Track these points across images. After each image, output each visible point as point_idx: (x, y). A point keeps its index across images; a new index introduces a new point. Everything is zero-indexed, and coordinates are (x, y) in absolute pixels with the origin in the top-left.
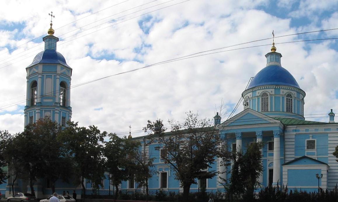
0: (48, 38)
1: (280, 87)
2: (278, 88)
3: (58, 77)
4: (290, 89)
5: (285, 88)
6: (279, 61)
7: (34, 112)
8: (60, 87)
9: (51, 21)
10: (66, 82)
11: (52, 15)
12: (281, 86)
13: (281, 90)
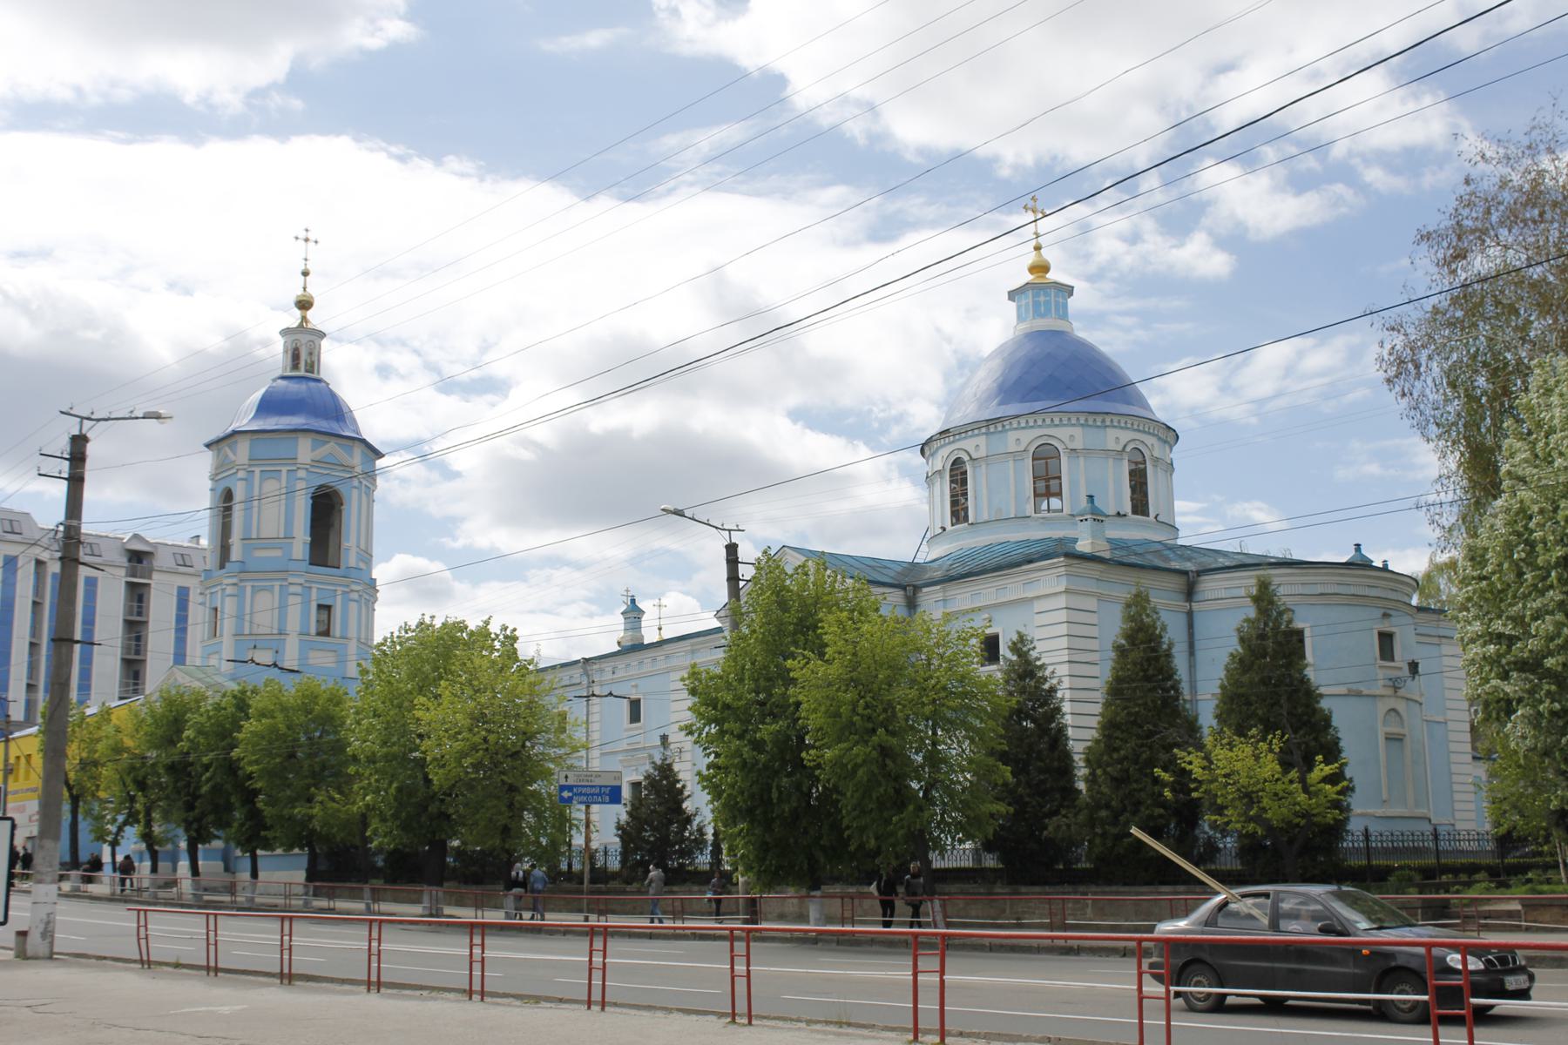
2: (1000, 429)
5: (1023, 425)
6: (1063, 314)
7: (219, 593)
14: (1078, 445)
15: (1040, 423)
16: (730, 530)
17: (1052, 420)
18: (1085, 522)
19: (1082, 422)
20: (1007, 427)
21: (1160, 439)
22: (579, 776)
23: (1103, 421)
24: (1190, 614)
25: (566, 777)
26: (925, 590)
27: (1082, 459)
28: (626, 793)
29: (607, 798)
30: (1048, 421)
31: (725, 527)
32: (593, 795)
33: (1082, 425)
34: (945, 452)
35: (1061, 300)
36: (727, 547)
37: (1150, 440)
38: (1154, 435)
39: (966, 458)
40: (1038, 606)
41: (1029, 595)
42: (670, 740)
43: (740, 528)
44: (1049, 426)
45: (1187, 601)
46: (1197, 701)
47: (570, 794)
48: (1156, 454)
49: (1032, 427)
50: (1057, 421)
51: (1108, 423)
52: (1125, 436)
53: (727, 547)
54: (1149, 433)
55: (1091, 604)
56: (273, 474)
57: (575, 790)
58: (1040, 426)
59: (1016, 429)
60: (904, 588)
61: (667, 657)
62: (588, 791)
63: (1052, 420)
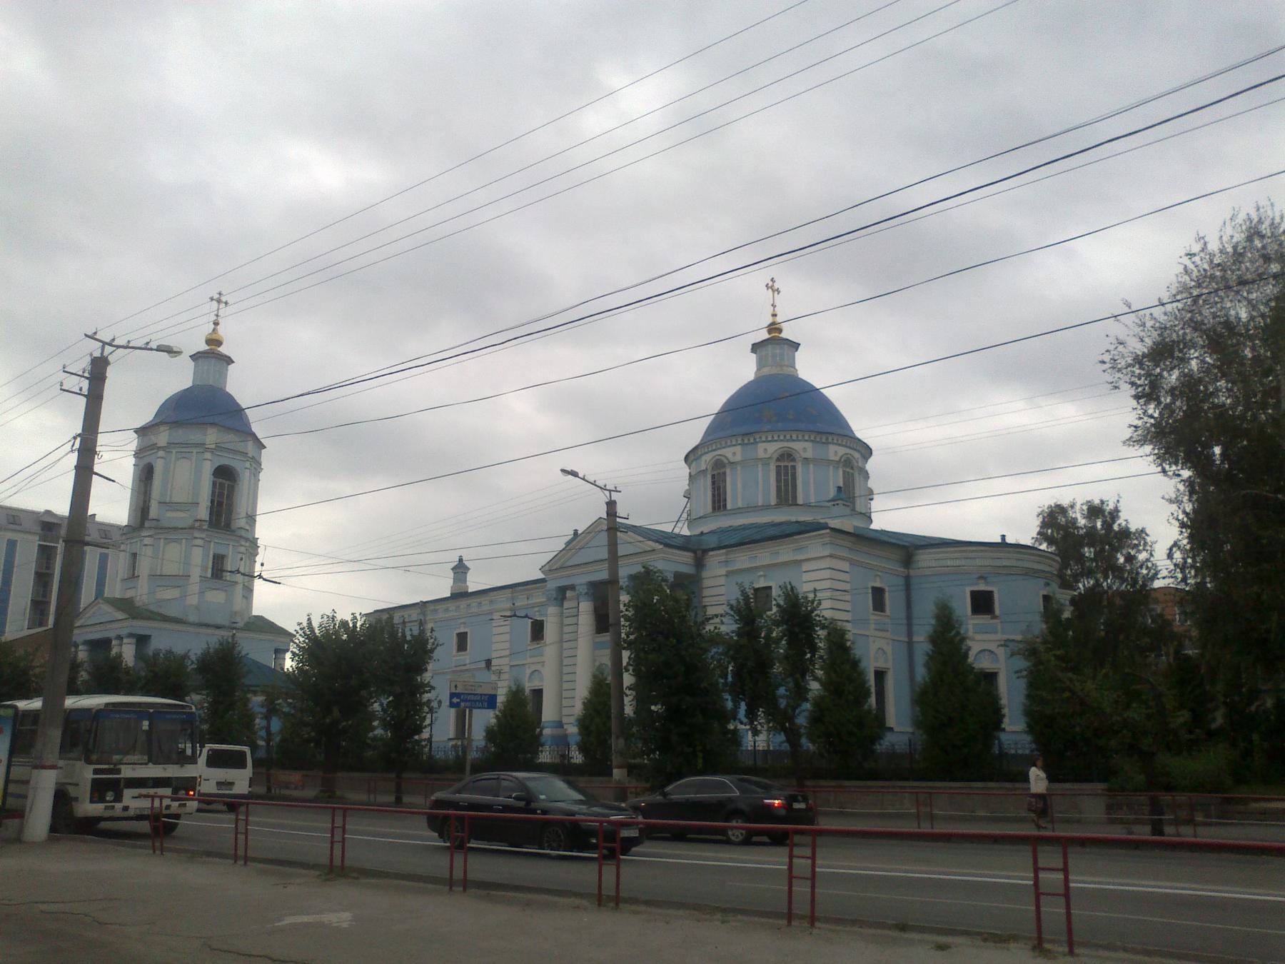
0: (200, 357)
1: (755, 439)
2: (752, 441)
3: (208, 455)
5: (770, 439)
7: (139, 543)
8: (215, 479)
9: (217, 316)
10: (238, 469)
11: (219, 301)
12: (757, 436)
13: (760, 445)
14: (809, 454)
15: (782, 438)
16: (610, 491)
17: (791, 437)
18: (836, 506)
19: (812, 438)
20: (758, 440)
22: (465, 685)
23: (827, 439)
24: (908, 579)
25: (456, 686)
26: (711, 553)
27: (811, 466)
28: (501, 699)
29: (486, 704)
30: (788, 437)
31: (608, 488)
32: (475, 701)
33: (812, 441)
34: (708, 457)
36: (607, 503)
37: (857, 455)
39: (726, 461)
40: (806, 567)
41: (800, 557)
42: (493, 663)
43: (618, 489)
44: (788, 441)
46: (913, 642)
47: (458, 700)
49: (776, 441)
50: (794, 437)
52: (842, 451)
53: (607, 503)
55: (845, 566)
56: (184, 455)
57: (462, 697)
58: (782, 441)
59: (764, 442)
60: (694, 551)
61: (491, 602)
62: (472, 698)
63: (791, 437)
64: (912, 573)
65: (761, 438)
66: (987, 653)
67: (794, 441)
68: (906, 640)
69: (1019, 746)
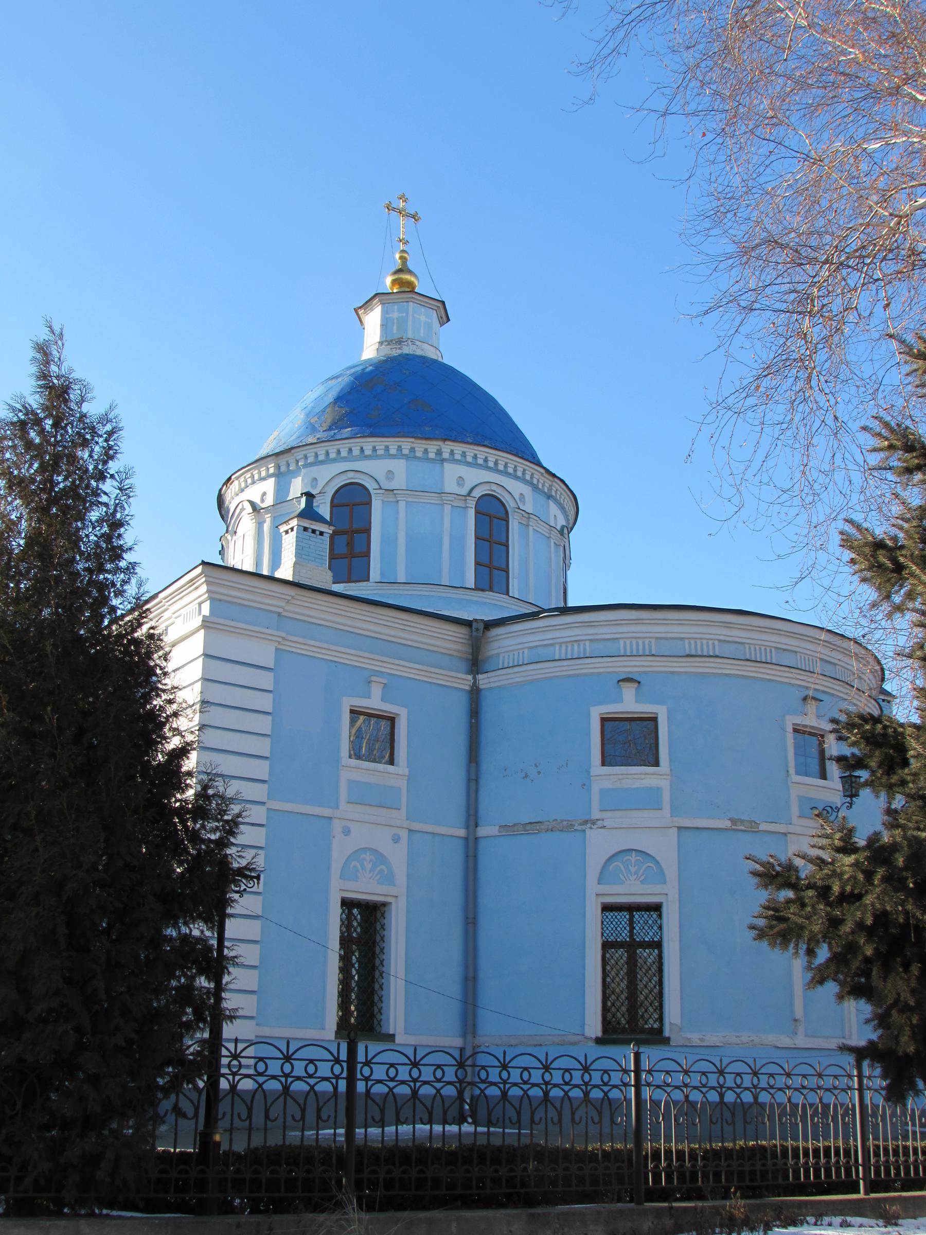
4: (356, 452)
14: (399, 482)
17: (362, 450)
21: (535, 487)
24: (475, 695)
33: (407, 457)
35: (423, 318)
38: (523, 480)
44: (356, 459)
45: (470, 672)
46: (476, 839)
48: (528, 507)
51: (446, 455)
52: (473, 476)
54: (516, 478)
55: (264, 654)
64: (483, 680)
65: (306, 457)
66: (633, 858)
67: (368, 457)
68: (462, 833)
69: (557, 1078)
